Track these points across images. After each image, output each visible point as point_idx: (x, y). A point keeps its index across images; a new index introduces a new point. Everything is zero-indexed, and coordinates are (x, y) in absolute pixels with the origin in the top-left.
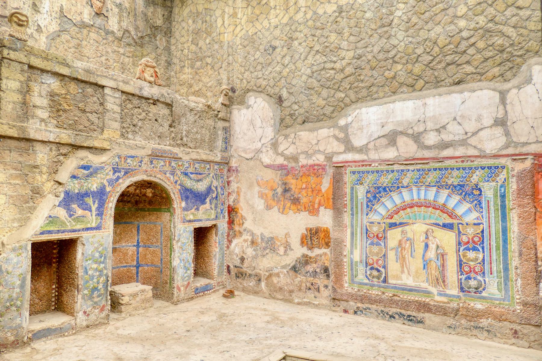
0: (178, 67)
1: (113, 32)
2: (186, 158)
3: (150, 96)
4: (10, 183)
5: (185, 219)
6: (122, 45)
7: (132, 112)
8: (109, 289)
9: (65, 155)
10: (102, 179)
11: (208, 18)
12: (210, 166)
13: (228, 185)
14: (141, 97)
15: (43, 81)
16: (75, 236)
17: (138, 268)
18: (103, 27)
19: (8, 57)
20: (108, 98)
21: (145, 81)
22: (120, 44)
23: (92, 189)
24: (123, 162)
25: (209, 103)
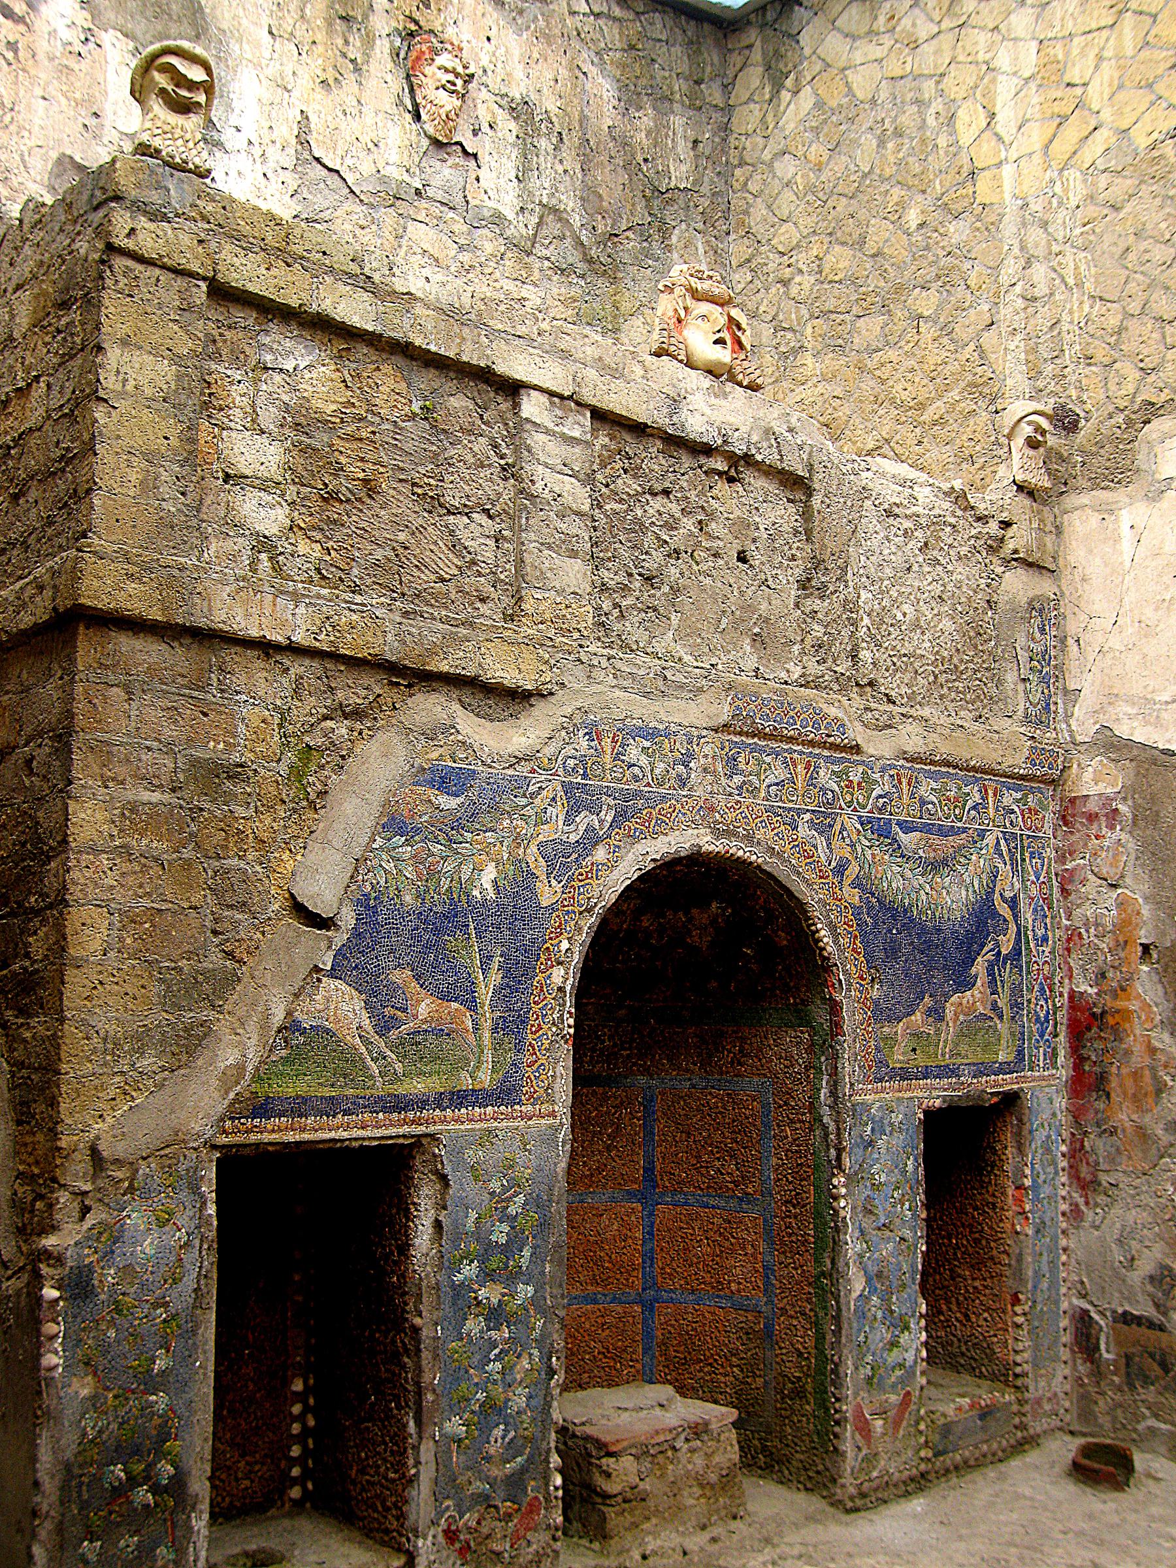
0: (769, 360)
1: (498, 219)
2: (878, 746)
3: (712, 437)
4: (125, 851)
5: (882, 1063)
6: (536, 274)
7: (639, 512)
8: (556, 1415)
9: (356, 714)
10: (518, 840)
11: (908, 119)
12: (984, 791)
13: (1065, 892)
14: (676, 443)
15: (268, 358)
16: (405, 1130)
17: (649, 1307)
18: (458, 200)
19: (130, 244)
20: (537, 440)
21: (690, 364)
22: (527, 266)
23: (476, 893)
24: (608, 759)
25: (957, 484)
